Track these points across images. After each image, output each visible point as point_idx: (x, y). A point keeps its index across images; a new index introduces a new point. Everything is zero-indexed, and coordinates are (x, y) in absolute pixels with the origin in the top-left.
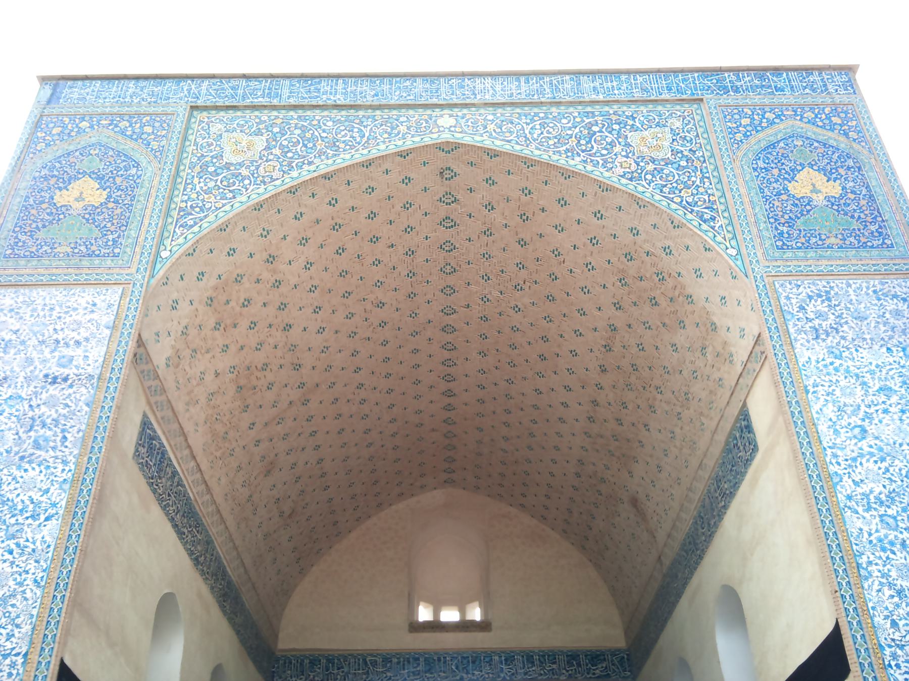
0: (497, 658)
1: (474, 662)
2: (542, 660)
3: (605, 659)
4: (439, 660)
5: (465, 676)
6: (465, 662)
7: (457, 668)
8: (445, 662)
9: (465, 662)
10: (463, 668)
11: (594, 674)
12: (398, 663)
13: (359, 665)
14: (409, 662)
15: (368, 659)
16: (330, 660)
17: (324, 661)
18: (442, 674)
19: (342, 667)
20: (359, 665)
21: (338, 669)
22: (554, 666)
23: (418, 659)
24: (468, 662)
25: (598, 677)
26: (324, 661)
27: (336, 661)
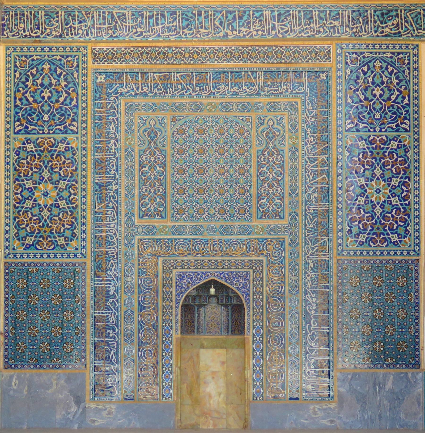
0: (268, 12)
1: (240, 18)
2: (322, 15)
3: (397, 16)
4: (200, 14)
5: (229, 32)
6: (230, 17)
7: (221, 23)
8: (206, 17)
9: (230, 17)
10: (228, 25)
11: (383, 32)
12: (151, 17)
13: (104, 18)
14: (163, 16)
15: (114, 12)
16: (70, 13)
17: (62, 14)
18: (203, 30)
19: (84, 21)
20: (104, 18)
21: (80, 22)
22: (336, 23)
23: (174, 13)
24: (235, 16)
25: (386, 36)
26: (62, 14)
27: (77, 13)
